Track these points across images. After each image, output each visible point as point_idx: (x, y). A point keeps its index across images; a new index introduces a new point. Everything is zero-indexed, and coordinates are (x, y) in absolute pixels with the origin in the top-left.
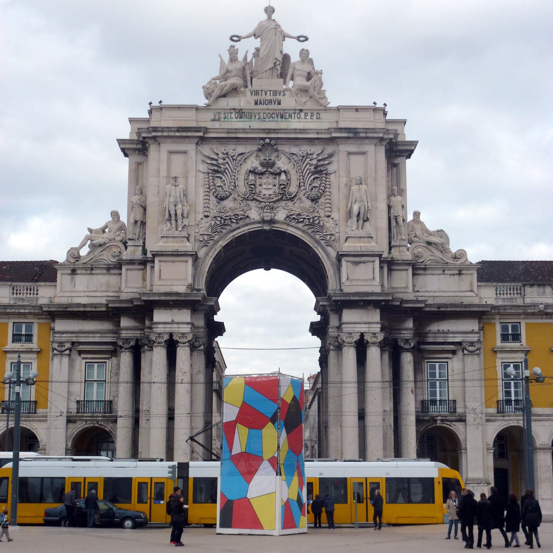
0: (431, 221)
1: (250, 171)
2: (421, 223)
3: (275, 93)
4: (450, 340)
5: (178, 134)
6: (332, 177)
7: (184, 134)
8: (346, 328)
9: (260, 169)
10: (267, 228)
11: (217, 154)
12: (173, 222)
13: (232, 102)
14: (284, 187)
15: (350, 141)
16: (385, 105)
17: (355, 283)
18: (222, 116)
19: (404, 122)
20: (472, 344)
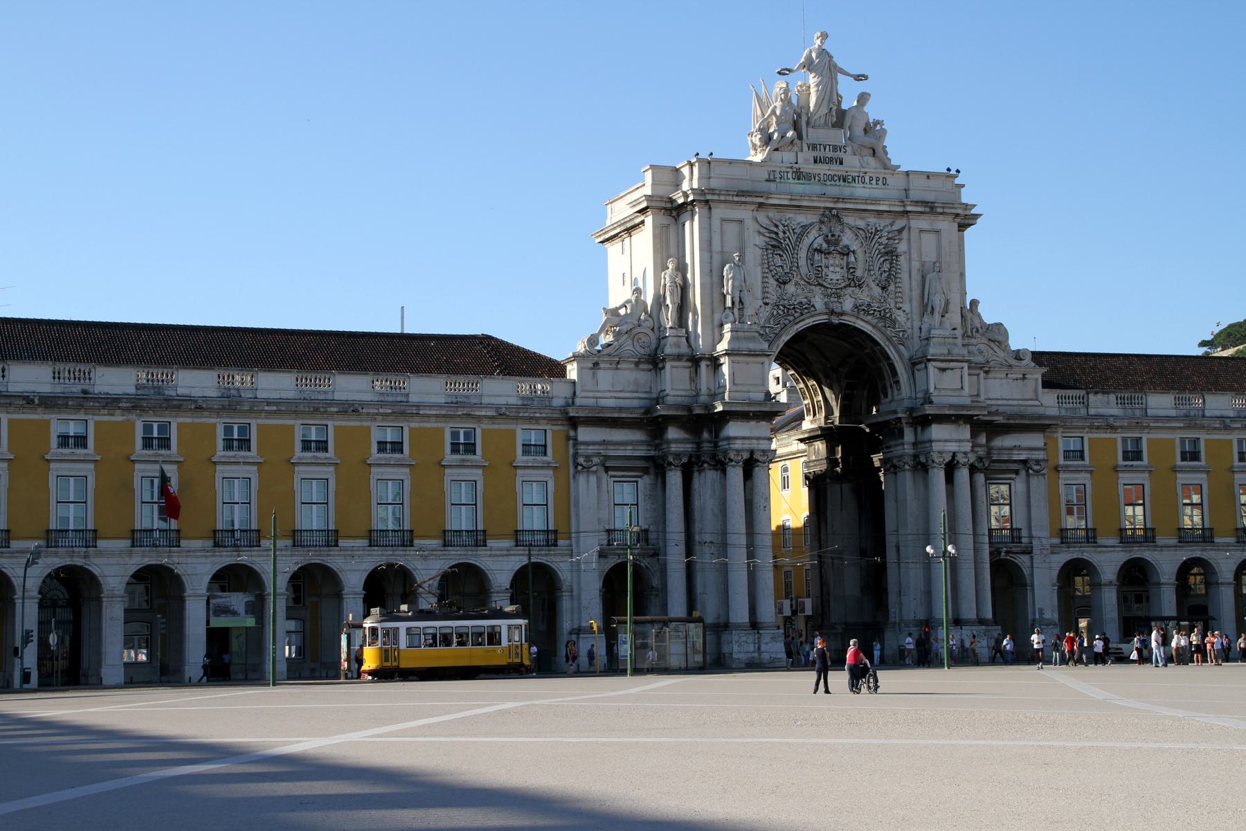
0: (989, 315)
1: (816, 250)
2: (979, 316)
3: (835, 148)
4: (1015, 458)
5: (736, 199)
6: (902, 259)
7: (743, 199)
8: (936, 447)
9: (825, 245)
10: (835, 320)
11: (777, 226)
12: (736, 310)
13: (788, 156)
14: (850, 269)
15: (923, 216)
16: (958, 171)
17: (943, 393)
18: (778, 176)
19: (963, 186)
20: (1038, 462)
